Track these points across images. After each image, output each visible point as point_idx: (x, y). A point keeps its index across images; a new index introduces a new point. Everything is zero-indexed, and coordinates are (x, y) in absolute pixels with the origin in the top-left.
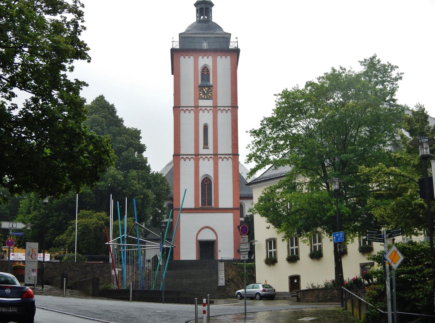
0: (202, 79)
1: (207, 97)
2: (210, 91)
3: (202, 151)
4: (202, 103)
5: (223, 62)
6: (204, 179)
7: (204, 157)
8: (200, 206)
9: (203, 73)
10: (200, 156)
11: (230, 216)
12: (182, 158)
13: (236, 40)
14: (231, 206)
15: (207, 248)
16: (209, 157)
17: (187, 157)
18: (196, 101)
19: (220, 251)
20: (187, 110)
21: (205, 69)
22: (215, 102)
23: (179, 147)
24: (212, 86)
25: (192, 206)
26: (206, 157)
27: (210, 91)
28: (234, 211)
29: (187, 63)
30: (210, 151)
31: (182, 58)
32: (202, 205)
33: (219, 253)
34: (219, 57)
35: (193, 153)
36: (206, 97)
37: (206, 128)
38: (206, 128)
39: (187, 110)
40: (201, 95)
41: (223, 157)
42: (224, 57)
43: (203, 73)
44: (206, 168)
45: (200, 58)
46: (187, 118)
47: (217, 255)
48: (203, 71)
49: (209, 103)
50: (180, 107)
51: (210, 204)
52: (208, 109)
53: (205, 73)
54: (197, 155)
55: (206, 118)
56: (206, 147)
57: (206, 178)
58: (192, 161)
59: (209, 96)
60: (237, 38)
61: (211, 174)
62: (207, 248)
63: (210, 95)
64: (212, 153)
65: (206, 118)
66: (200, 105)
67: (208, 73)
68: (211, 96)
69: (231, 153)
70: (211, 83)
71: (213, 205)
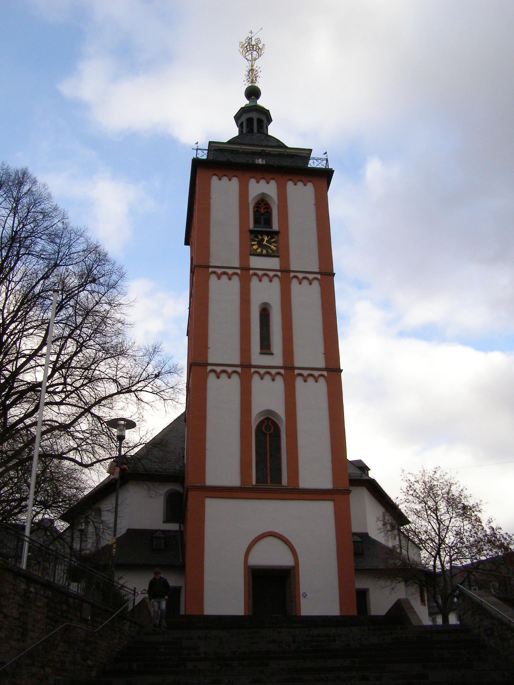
0: (257, 221)
1: (267, 251)
2: (274, 242)
3: (257, 358)
4: (255, 262)
5: (300, 193)
6: (262, 422)
7: (262, 371)
8: (254, 482)
9: (257, 211)
10: (253, 370)
11: (327, 508)
12: (213, 371)
13: (324, 157)
15: (272, 586)
16: (273, 371)
17: (224, 371)
19: (305, 595)
20: (225, 273)
21: (262, 207)
22: (285, 258)
23: (205, 348)
24: (277, 233)
26: (268, 373)
29: (225, 192)
30: (276, 359)
31: (214, 180)
32: (257, 482)
33: (303, 601)
35: (237, 362)
36: (264, 252)
40: (255, 247)
42: (300, 184)
44: (268, 396)
45: (253, 182)
46: (224, 293)
47: (297, 605)
48: (257, 207)
49: (274, 263)
50: (209, 267)
51: (277, 477)
52: (271, 274)
54: (246, 370)
55: (265, 292)
56: (265, 351)
57: (268, 419)
58: (236, 379)
60: (326, 153)
62: (272, 586)
65: (265, 292)
67: (268, 212)
68: (277, 250)
70: (275, 227)
71: (285, 481)
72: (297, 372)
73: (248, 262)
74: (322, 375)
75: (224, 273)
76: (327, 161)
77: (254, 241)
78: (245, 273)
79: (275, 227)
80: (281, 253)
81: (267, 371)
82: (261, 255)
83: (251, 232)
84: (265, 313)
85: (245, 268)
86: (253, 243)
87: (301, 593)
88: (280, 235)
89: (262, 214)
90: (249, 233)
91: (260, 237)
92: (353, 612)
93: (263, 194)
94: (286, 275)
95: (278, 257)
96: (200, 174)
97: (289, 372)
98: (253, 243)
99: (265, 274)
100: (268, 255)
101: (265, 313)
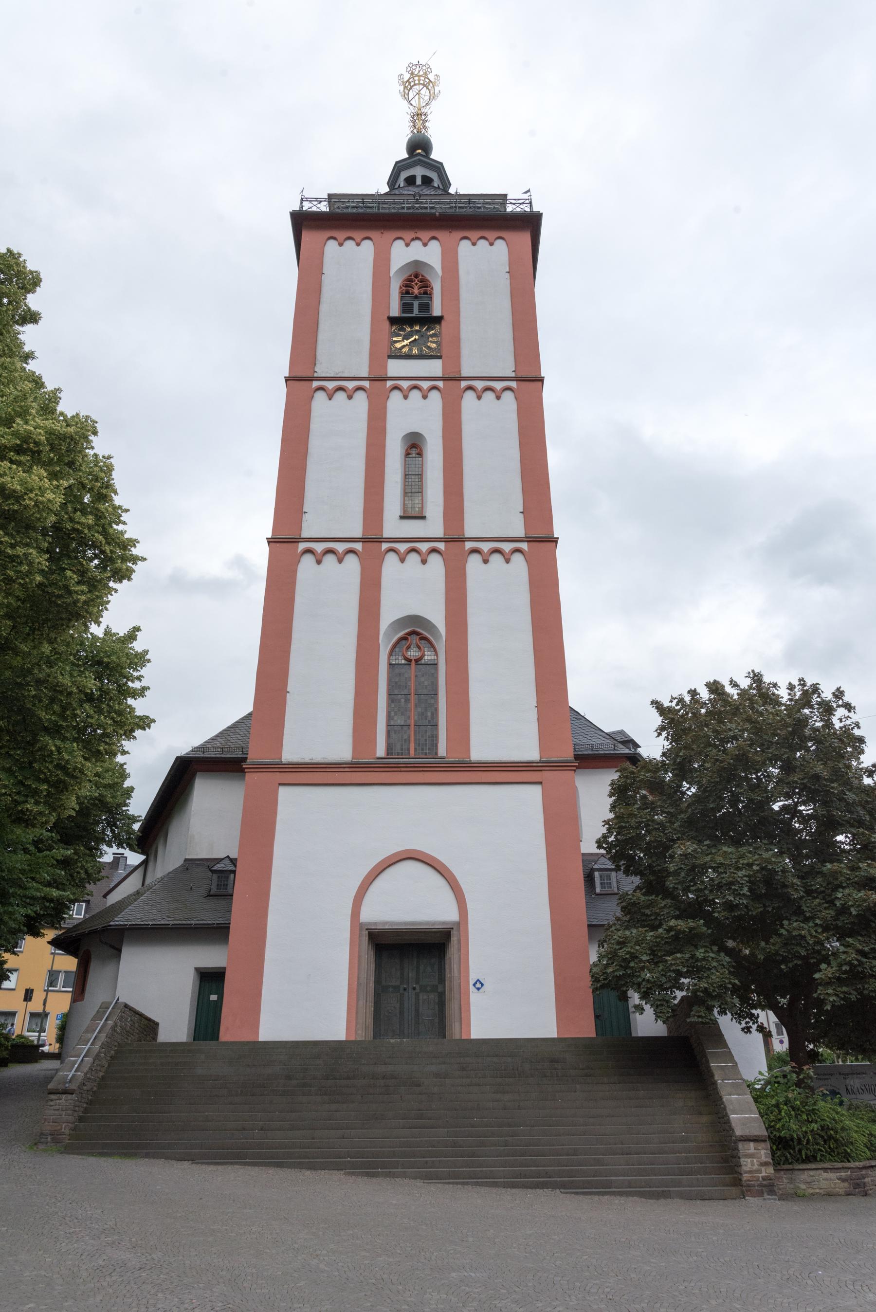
1: (420, 350)
2: (432, 336)
3: (393, 526)
5: (482, 260)
7: (402, 547)
8: (381, 751)
9: (407, 293)
10: (385, 546)
13: (526, 196)
14: (533, 754)
15: (410, 963)
16: (424, 547)
17: (329, 549)
19: (479, 985)
20: (341, 389)
23: (300, 512)
24: (438, 320)
25: (343, 752)
27: (432, 336)
28: (547, 775)
33: (475, 998)
34: (465, 245)
35: (358, 533)
37: (414, 445)
38: (414, 445)
39: (341, 389)
41: (486, 547)
43: (407, 293)
44: (413, 589)
46: (338, 423)
53: (416, 291)
54: (372, 544)
58: (352, 563)
59: (429, 348)
60: (529, 191)
61: (437, 616)
62: (410, 963)
63: (434, 346)
64: (440, 533)
65: (414, 414)
66: (390, 374)
67: (425, 293)
69: (520, 532)
71: (442, 751)
72: (469, 545)
74: (518, 550)
76: (531, 203)
78: (378, 384)
79: (436, 311)
81: (412, 547)
82: (409, 357)
83: (393, 321)
85: (378, 379)
86: (395, 339)
87: (471, 983)
88: (443, 323)
89: (416, 297)
90: (388, 323)
91: (409, 329)
92: (585, 1028)
93: (417, 263)
94: (453, 383)
95: (440, 357)
96: (306, 236)
97: (455, 545)
98: (395, 339)
99: (417, 385)
100: (420, 357)
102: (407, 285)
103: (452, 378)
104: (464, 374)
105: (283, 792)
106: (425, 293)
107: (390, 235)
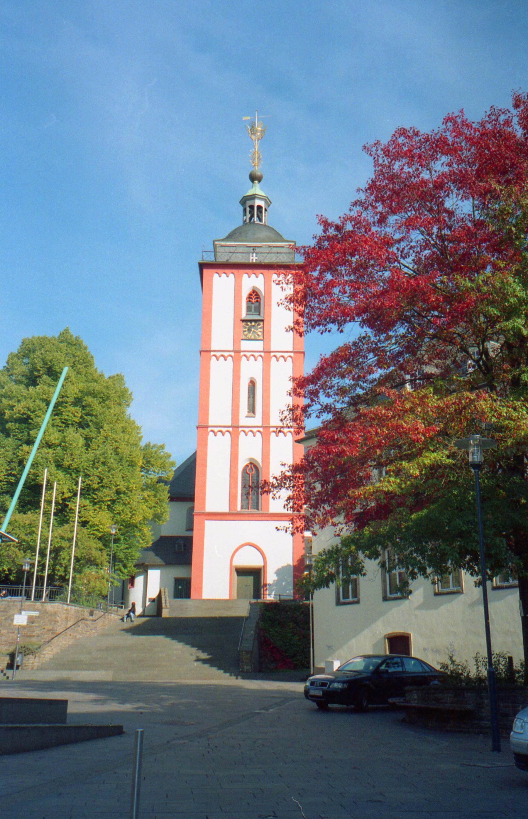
1: (255, 336)
3: (243, 421)
4: (245, 345)
8: (239, 508)
10: (240, 429)
12: (212, 431)
16: (255, 430)
18: (236, 341)
25: (226, 510)
30: (257, 420)
32: (242, 508)
35: (230, 424)
49: (258, 345)
54: (235, 429)
55: (251, 369)
61: (258, 458)
66: (242, 349)
72: (272, 429)
73: (239, 345)
75: (222, 355)
77: (245, 328)
80: (265, 337)
83: (243, 321)
84: (252, 384)
85: (237, 352)
96: (205, 271)
101: (252, 384)
102: (250, 297)
103: (267, 352)
104: (272, 350)
105: (207, 522)
106: (257, 301)
107: (241, 271)
